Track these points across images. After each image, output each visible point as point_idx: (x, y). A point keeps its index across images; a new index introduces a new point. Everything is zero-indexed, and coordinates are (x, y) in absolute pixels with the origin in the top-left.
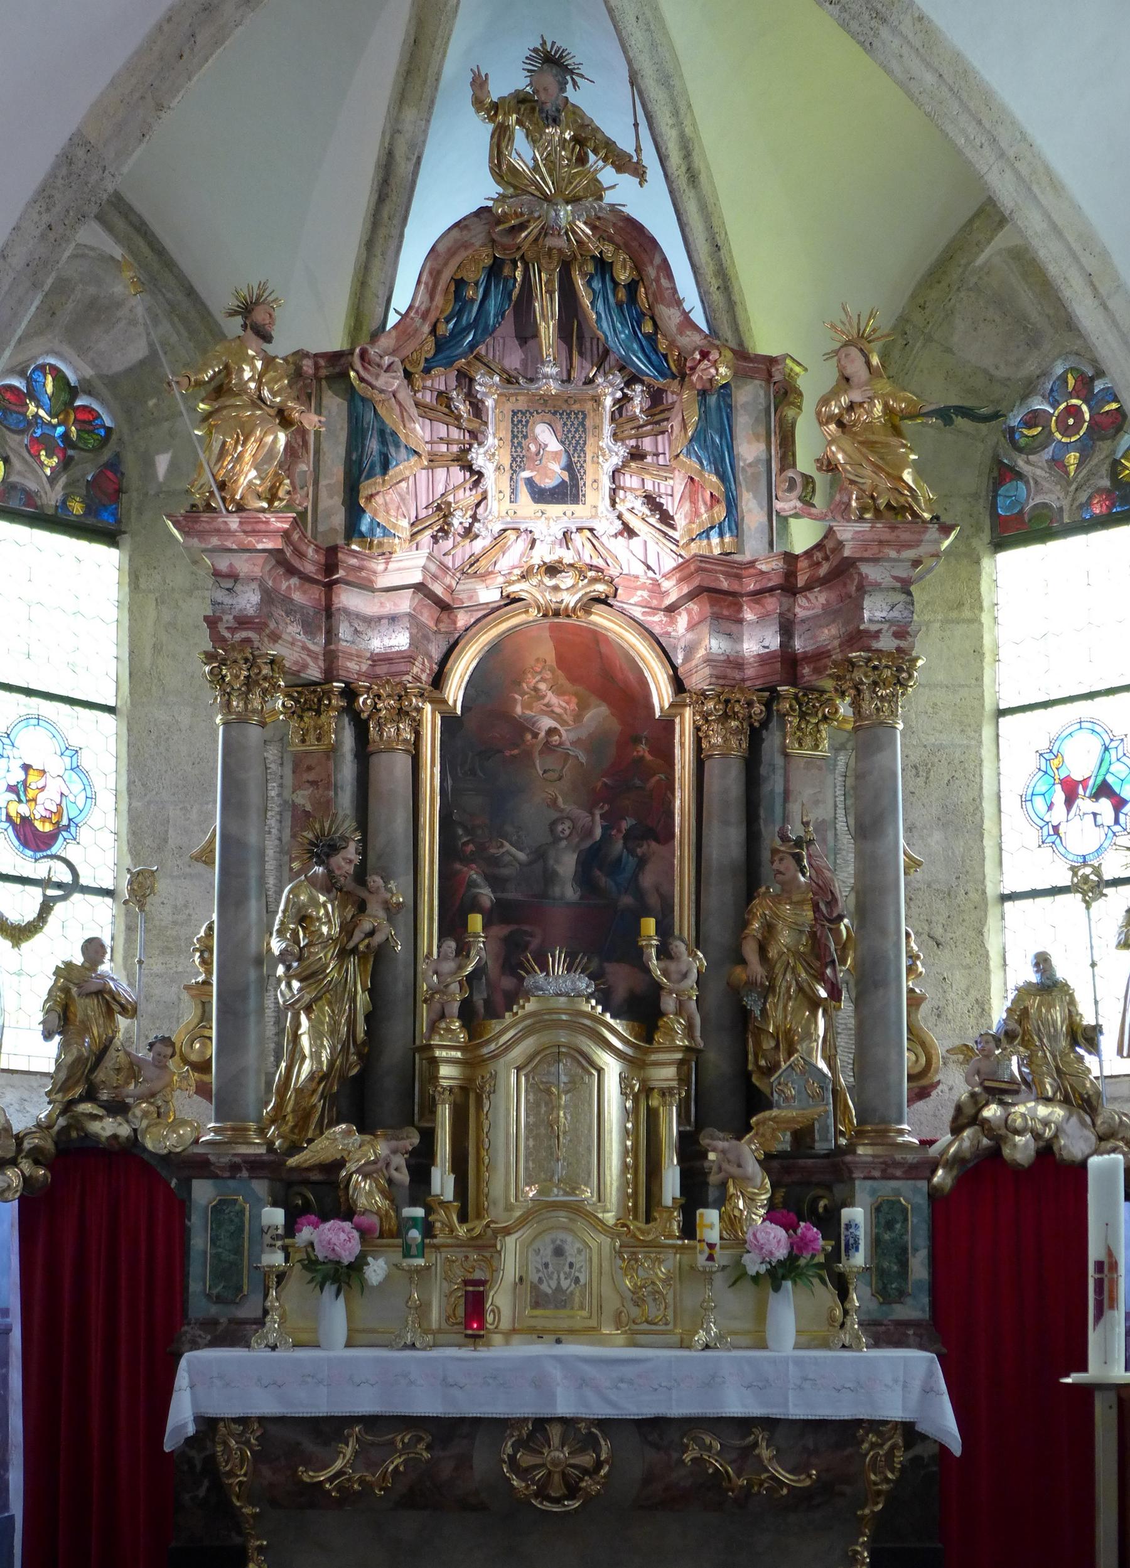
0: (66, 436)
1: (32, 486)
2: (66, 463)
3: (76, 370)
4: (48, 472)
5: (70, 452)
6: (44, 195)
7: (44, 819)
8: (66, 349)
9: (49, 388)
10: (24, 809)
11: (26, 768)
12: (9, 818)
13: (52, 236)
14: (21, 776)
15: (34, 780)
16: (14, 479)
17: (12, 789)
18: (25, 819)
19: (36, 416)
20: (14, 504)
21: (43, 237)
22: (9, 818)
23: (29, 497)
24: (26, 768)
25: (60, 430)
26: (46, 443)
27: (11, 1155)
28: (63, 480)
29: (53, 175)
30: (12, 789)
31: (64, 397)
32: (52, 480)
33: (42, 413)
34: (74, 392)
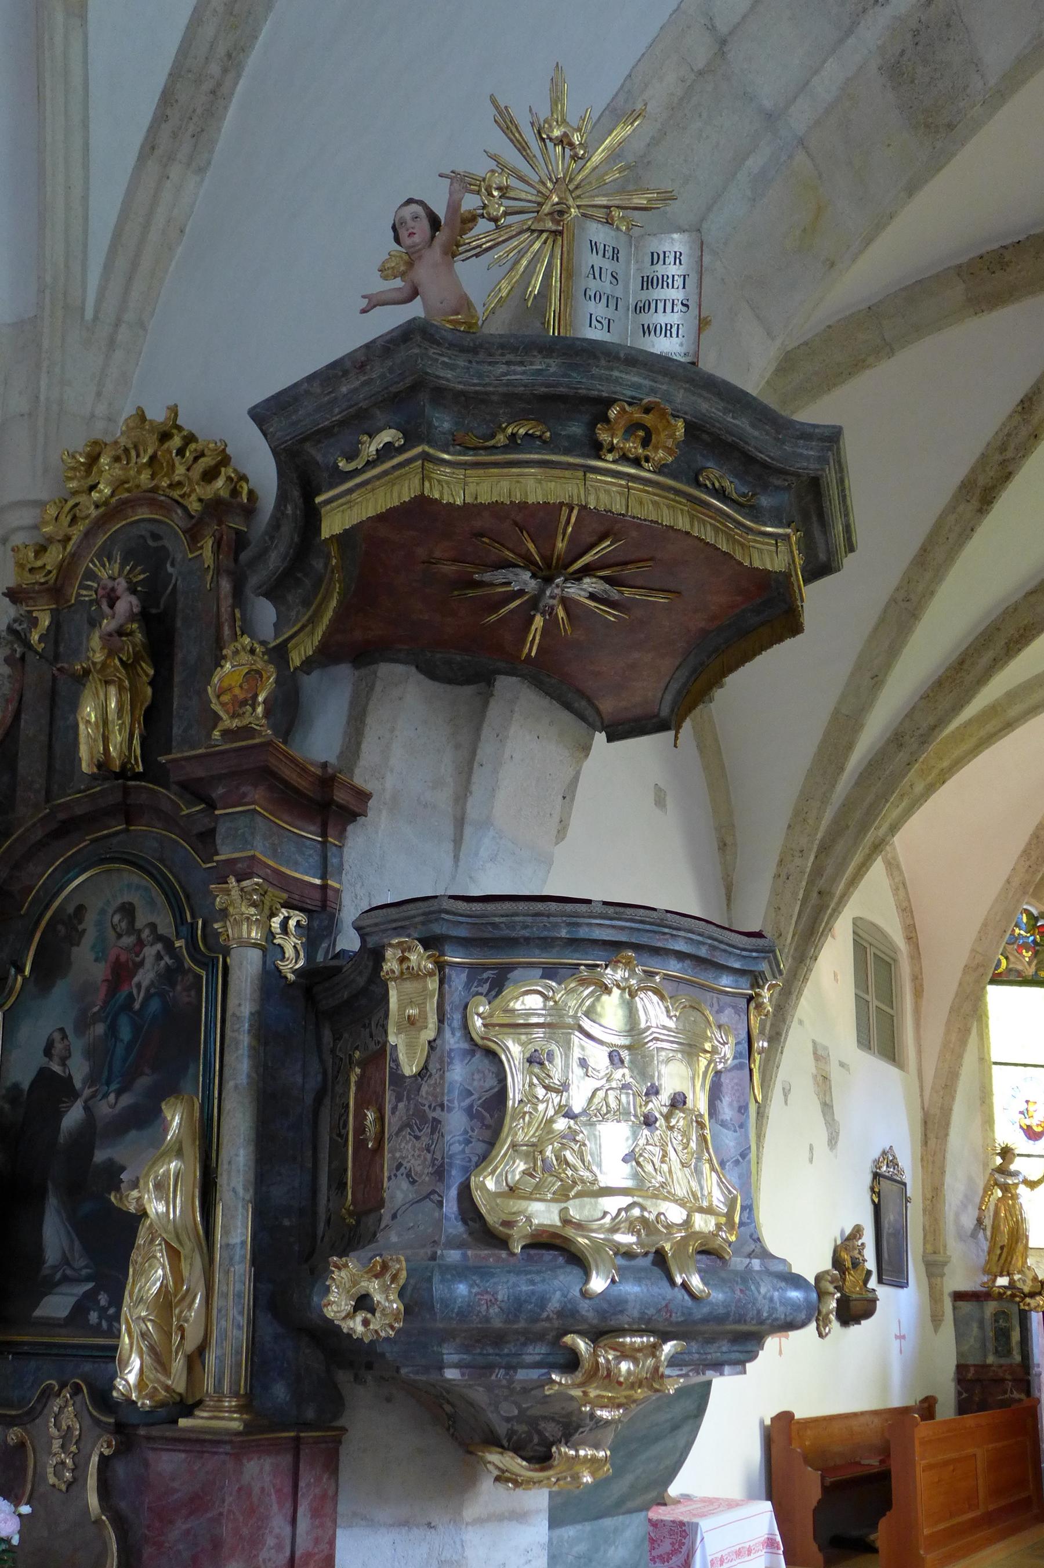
0: (1034, 941)
1: (1020, 967)
2: (1036, 954)
3: (1037, 908)
4: (1027, 959)
5: (1037, 948)
6: (1026, 853)
7: (1038, 1125)
8: (1033, 901)
9: (1025, 920)
10: (1028, 1122)
11: (1027, 1102)
12: (1021, 1127)
13: (1031, 870)
14: (1025, 1106)
15: (1031, 1107)
16: (1011, 966)
17: (1021, 1113)
18: (1028, 1126)
19: (1019, 934)
20: (1012, 978)
21: (1027, 871)
22: (1021, 1127)
23: (1019, 973)
24: (1027, 1102)
25: (1032, 938)
26: (1025, 946)
27: (1038, 1290)
28: (1035, 962)
29: (1029, 844)
30: (1021, 1113)
31: (1032, 922)
32: (1029, 963)
33: (1022, 932)
34: (1036, 919)
